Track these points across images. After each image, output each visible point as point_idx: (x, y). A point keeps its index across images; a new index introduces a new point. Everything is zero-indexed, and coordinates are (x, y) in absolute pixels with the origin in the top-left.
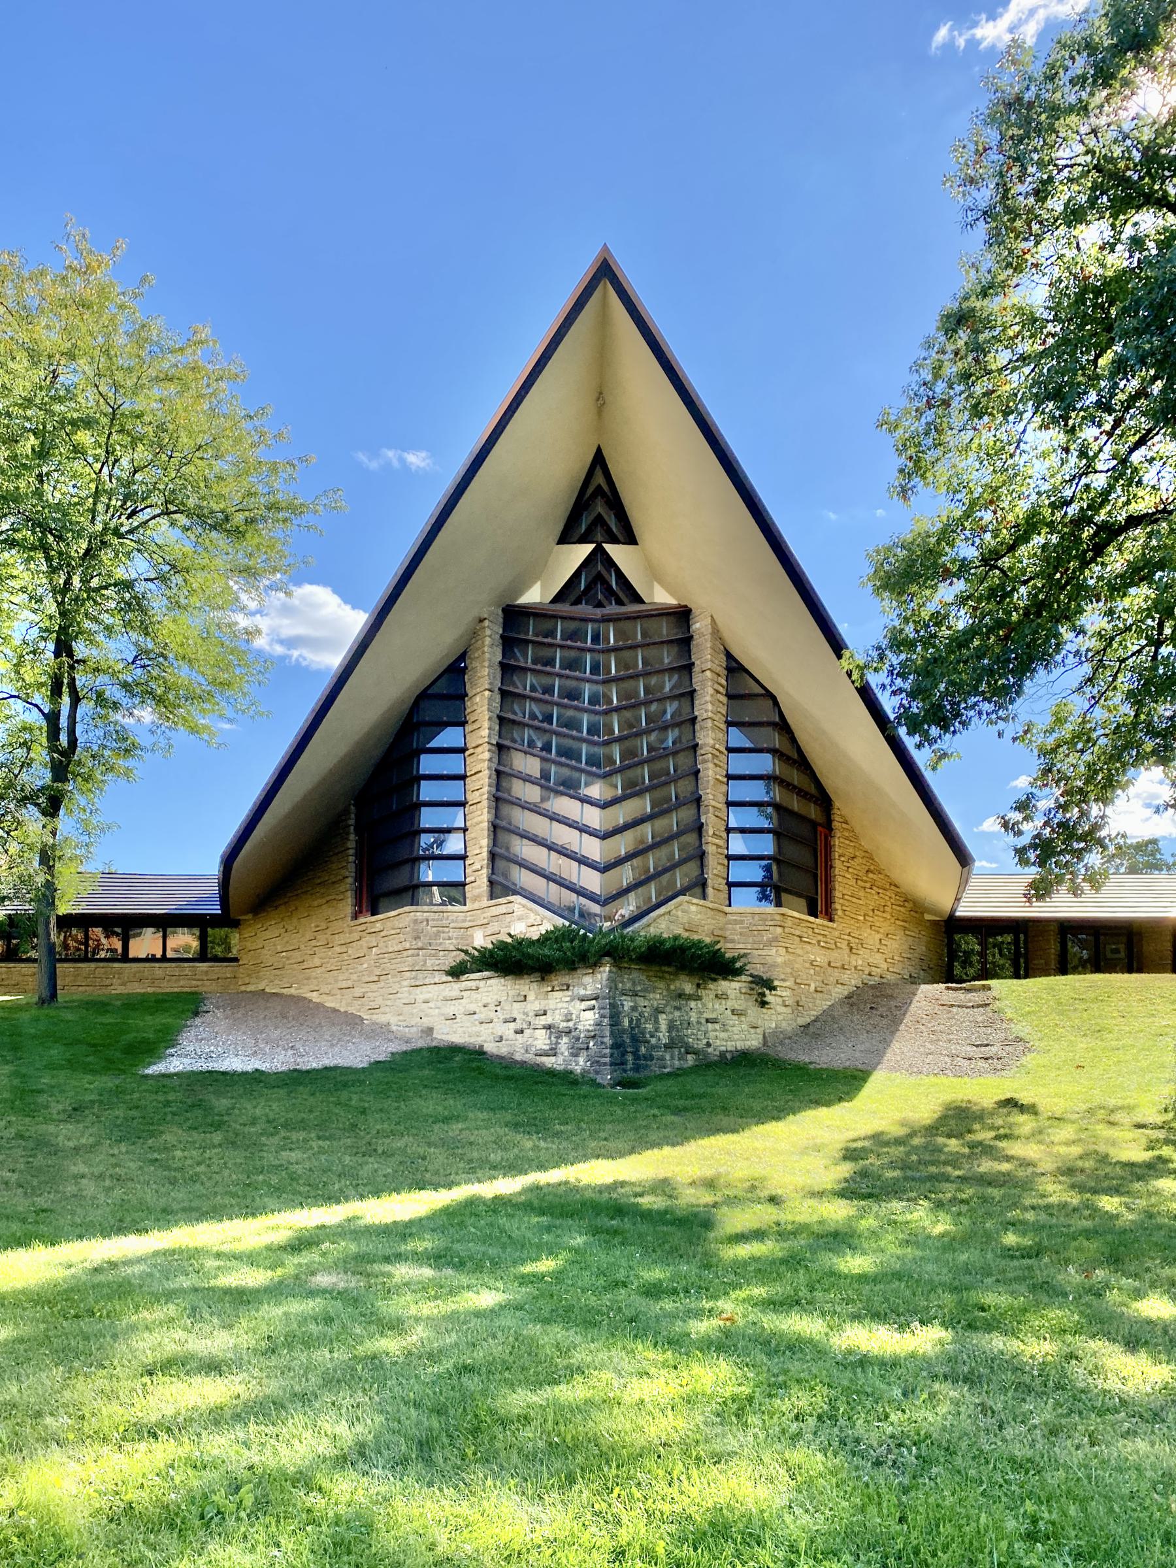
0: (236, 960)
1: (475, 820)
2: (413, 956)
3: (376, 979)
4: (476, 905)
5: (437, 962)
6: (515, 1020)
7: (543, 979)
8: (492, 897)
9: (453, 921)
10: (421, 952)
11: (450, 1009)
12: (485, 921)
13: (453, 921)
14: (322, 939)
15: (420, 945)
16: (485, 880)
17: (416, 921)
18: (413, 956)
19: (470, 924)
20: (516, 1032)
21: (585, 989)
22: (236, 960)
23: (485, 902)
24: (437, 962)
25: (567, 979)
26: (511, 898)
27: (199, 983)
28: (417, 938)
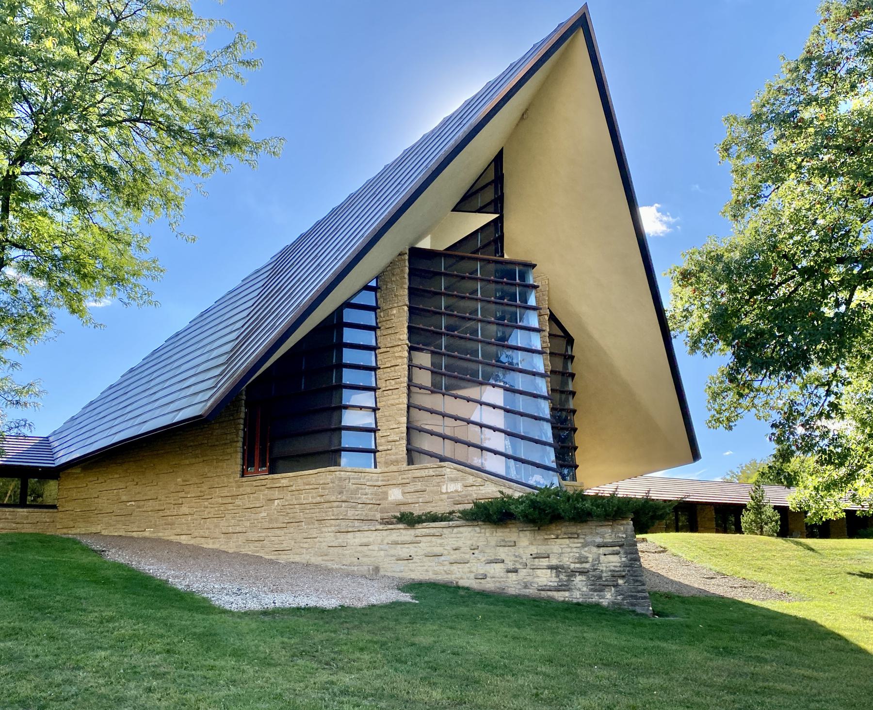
0: (54, 507)
1: (392, 402)
2: (337, 507)
3: (284, 525)
4: (394, 468)
5: (357, 513)
6: (503, 561)
7: (539, 529)
8: (410, 462)
9: (368, 480)
10: (344, 504)
11: (404, 552)
12: (407, 481)
13: (368, 480)
14: (193, 491)
15: (344, 498)
16: (405, 449)
17: (340, 479)
18: (337, 507)
19: (384, 483)
20: (509, 571)
21: (604, 537)
22: (54, 507)
23: (404, 466)
24: (357, 513)
25: (573, 529)
26: (442, 464)
27: (20, 526)
28: (341, 493)
